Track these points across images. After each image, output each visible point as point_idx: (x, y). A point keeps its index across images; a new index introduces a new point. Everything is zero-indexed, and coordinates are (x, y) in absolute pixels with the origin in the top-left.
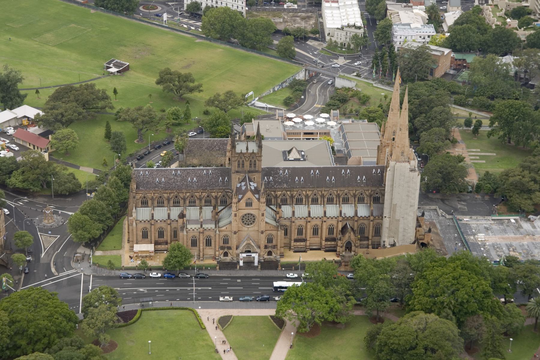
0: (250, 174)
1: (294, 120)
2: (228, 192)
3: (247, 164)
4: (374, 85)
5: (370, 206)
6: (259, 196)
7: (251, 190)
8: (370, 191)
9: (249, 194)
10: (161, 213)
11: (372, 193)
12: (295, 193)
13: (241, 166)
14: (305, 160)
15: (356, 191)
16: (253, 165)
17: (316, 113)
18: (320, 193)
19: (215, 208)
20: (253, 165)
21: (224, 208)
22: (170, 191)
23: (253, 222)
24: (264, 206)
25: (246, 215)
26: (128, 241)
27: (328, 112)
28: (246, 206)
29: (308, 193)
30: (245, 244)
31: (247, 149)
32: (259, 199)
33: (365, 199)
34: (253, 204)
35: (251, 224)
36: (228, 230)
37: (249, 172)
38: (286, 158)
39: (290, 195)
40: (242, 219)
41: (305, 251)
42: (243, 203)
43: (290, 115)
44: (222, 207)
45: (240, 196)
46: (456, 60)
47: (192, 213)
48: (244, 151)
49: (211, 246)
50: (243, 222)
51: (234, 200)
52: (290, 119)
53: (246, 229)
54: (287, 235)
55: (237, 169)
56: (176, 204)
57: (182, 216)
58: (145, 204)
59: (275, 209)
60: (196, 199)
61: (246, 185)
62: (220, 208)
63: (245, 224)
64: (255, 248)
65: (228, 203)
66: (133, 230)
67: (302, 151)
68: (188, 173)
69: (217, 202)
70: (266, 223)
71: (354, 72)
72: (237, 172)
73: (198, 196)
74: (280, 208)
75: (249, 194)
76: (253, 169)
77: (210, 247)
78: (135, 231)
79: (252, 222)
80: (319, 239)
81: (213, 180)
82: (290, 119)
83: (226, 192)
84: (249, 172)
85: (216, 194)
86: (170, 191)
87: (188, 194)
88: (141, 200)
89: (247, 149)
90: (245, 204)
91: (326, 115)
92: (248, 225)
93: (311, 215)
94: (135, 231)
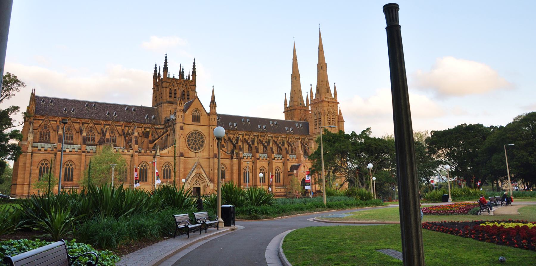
12: (232, 136)
13: (173, 95)
15: (289, 138)
22: (83, 121)
23: (202, 146)
25: (192, 134)
28: (193, 121)
29: (245, 137)
30: (194, 174)
34: (201, 118)
35: (199, 149)
36: (170, 154)
40: (188, 141)
48: (177, 77)
49: (146, 181)
53: (192, 154)
55: (168, 99)
60: (117, 135)
63: (192, 148)
64: (208, 181)
66: (25, 164)
72: (169, 102)
73: (120, 132)
77: (146, 183)
78: (28, 165)
79: (199, 146)
83: (156, 129)
85: (143, 130)
86: (83, 121)
88: (40, 129)
92: (195, 149)
94: (28, 165)
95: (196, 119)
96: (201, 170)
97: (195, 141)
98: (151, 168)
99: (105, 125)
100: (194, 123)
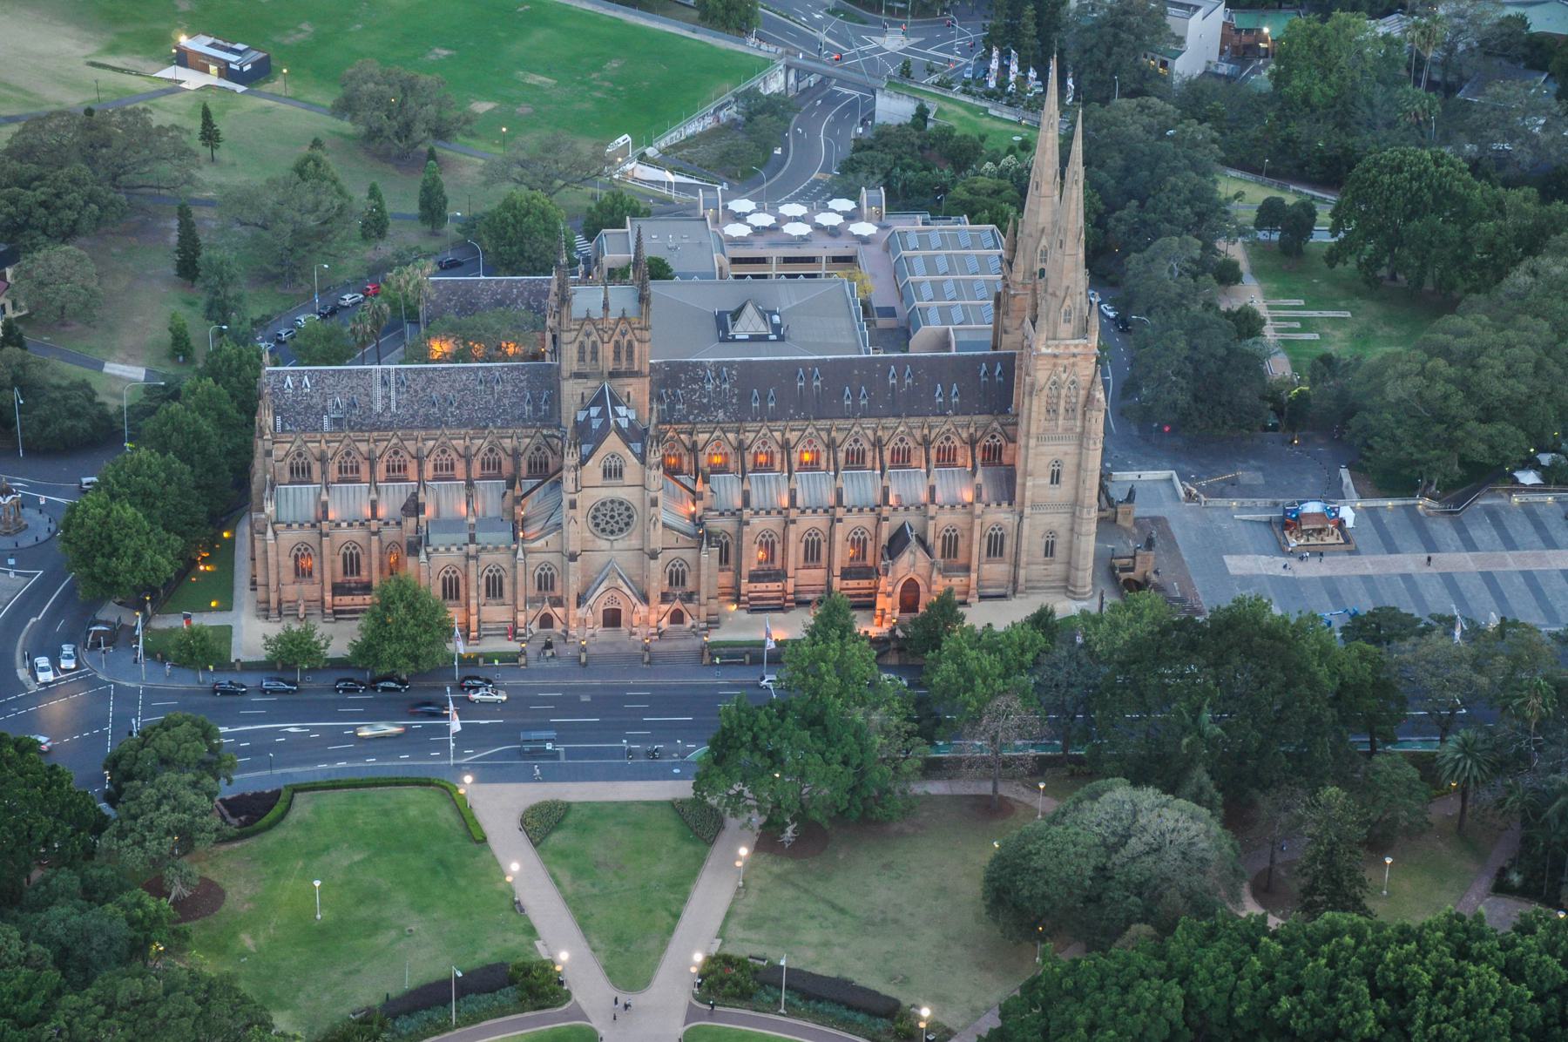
0: (617, 382)
1: (750, 219)
2: (553, 436)
3: (607, 351)
4: (992, 112)
5: (974, 473)
6: (644, 447)
7: (619, 430)
8: (972, 430)
9: (613, 442)
10: (348, 502)
11: (979, 434)
12: (752, 435)
13: (588, 357)
14: (781, 338)
15: (931, 428)
16: (624, 356)
17: (817, 197)
18: (825, 437)
19: (511, 484)
20: (624, 356)
21: (539, 485)
24: (656, 477)
25: (604, 504)
26: (254, 583)
27: (853, 195)
29: (787, 435)
31: (606, 306)
32: (642, 458)
33: (959, 452)
34: (625, 470)
37: (614, 375)
38: (726, 331)
39: (735, 444)
40: (595, 517)
41: (781, 609)
42: (594, 468)
43: (741, 205)
44: (535, 482)
45: (586, 448)
46: (1238, 31)
47: (445, 501)
48: (597, 313)
49: (501, 595)
50: (597, 525)
51: (571, 460)
52: (740, 218)
54: (727, 561)
55: (575, 368)
56: (396, 472)
57: (413, 507)
58: (300, 473)
59: (690, 484)
60: (454, 456)
61: (603, 414)
62: (529, 484)
63: (603, 530)
64: (635, 600)
65: (551, 471)
67: (775, 313)
68: (429, 380)
69: (517, 467)
70: (665, 525)
71: (931, 71)
73: (461, 450)
74: (706, 481)
75: (613, 442)
76: (624, 366)
78: (271, 554)
80: (318, 587)
81: (506, 401)
82: (740, 218)
83: (545, 437)
84: (614, 375)
85: (515, 442)
87: (431, 443)
88: (288, 460)
89: (606, 306)
90: (600, 471)
91: (847, 205)
92: (612, 532)
93: (799, 503)
95: (613, 473)
96: (620, 582)
97: (612, 517)
98: (510, 574)
99: (424, 440)
100: (608, 482)
